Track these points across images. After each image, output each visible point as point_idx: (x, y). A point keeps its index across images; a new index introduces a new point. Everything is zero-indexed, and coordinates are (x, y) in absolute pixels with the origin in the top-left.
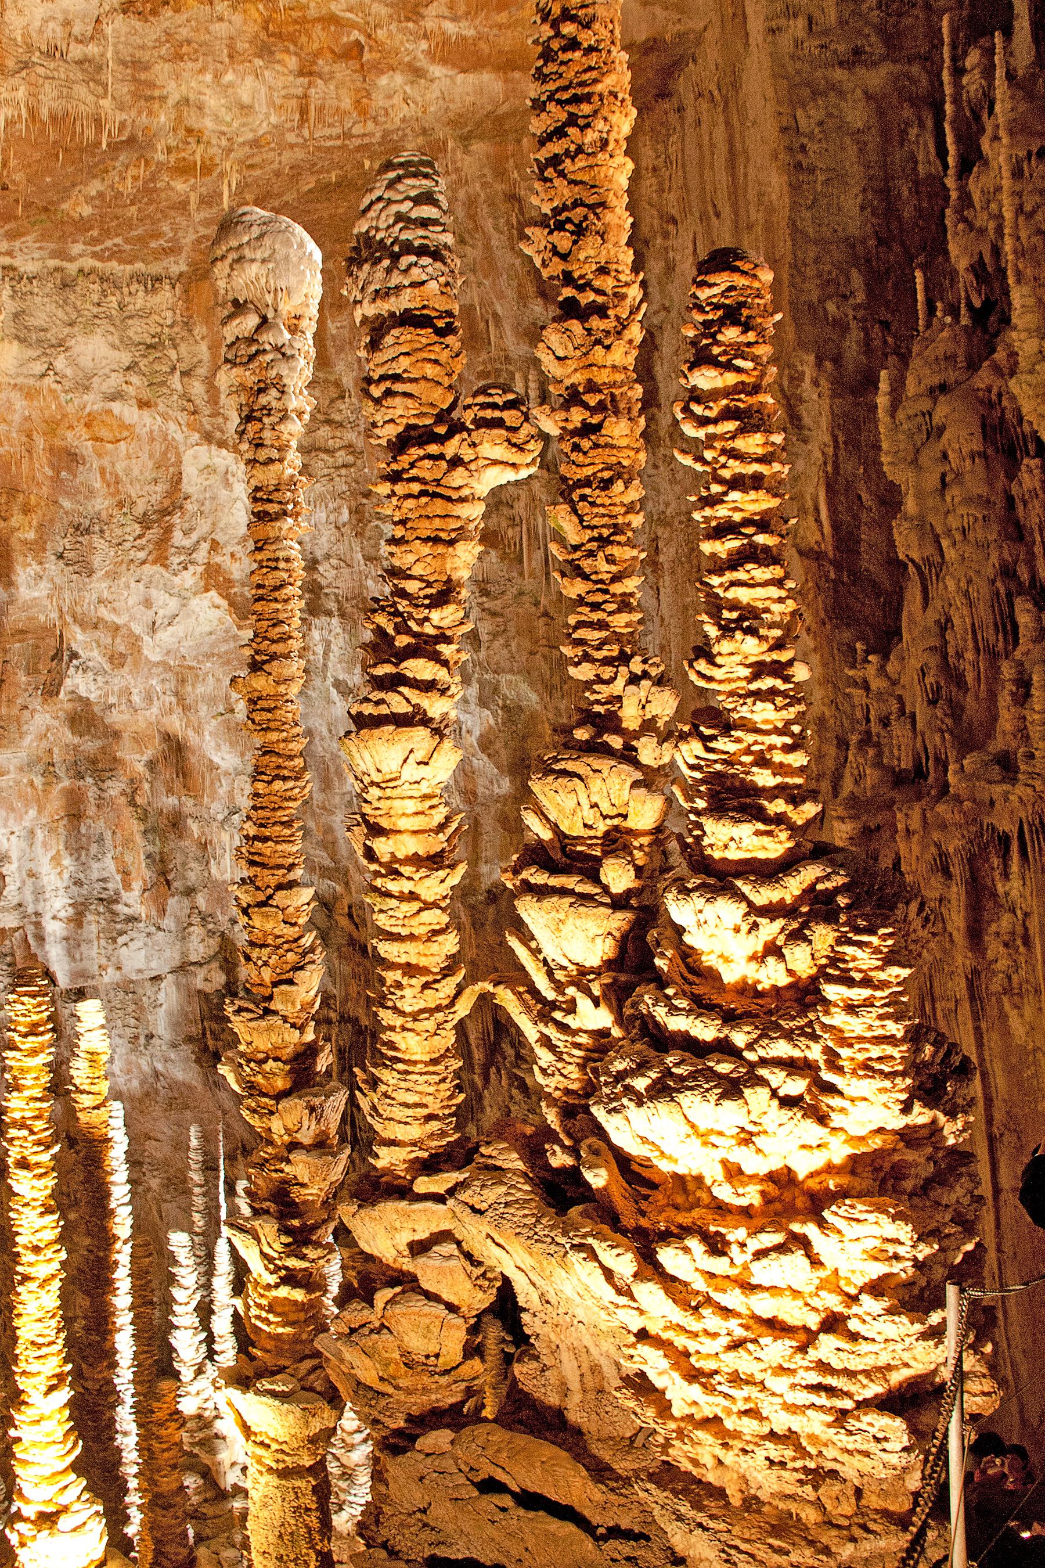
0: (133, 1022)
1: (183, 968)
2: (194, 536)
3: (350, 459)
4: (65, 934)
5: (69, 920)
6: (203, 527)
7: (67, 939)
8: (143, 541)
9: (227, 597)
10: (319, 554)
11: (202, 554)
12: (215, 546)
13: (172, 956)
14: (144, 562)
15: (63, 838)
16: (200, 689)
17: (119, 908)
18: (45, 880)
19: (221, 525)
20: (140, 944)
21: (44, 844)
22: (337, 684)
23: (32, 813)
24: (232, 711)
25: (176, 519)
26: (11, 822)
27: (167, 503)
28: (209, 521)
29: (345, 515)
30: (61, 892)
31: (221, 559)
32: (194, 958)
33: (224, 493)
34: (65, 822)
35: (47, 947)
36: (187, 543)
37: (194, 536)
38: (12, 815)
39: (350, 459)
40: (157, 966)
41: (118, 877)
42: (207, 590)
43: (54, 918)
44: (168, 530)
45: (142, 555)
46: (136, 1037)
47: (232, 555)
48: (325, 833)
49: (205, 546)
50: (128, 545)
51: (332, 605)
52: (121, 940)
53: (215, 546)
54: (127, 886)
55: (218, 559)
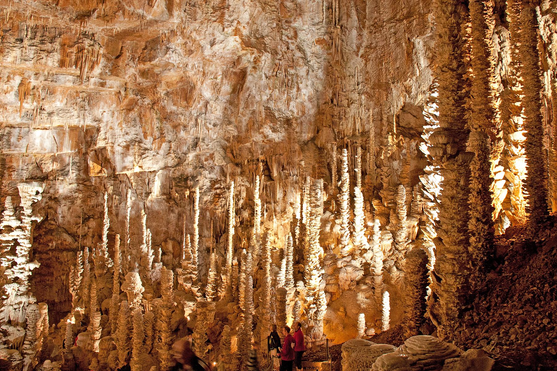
0: (140, 188)
1: (166, 168)
2: (232, 18)
3: (276, 10)
4: (122, 152)
5: (124, 147)
6: (235, 16)
7: (123, 154)
8: (214, 15)
9: (241, 39)
10: (264, 35)
11: (235, 23)
12: (239, 23)
13: (161, 164)
14: (215, 21)
15: (123, 117)
16: (210, 69)
17: (142, 145)
18: (116, 131)
19: (240, 17)
20: (151, 158)
21: (117, 118)
22: (265, 74)
23: (114, 105)
24: (216, 78)
25: (226, 11)
26: (105, 107)
27: (220, 5)
28: (237, 15)
29: (275, 25)
30: (121, 136)
31: (241, 27)
32: (169, 165)
33: (242, 8)
34: (125, 111)
35: (115, 156)
36: (230, 19)
37: (232, 18)
38: (106, 105)
39: (276, 10)
40: (155, 167)
41: (142, 134)
42: (235, 35)
43: (119, 145)
44: (223, 14)
45: (214, 19)
46: (142, 194)
47: (244, 27)
48: (239, 123)
49: (236, 22)
50: (209, 14)
51: (269, 50)
52: (144, 156)
53: (239, 23)
54: (146, 137)
55: (240, 27)
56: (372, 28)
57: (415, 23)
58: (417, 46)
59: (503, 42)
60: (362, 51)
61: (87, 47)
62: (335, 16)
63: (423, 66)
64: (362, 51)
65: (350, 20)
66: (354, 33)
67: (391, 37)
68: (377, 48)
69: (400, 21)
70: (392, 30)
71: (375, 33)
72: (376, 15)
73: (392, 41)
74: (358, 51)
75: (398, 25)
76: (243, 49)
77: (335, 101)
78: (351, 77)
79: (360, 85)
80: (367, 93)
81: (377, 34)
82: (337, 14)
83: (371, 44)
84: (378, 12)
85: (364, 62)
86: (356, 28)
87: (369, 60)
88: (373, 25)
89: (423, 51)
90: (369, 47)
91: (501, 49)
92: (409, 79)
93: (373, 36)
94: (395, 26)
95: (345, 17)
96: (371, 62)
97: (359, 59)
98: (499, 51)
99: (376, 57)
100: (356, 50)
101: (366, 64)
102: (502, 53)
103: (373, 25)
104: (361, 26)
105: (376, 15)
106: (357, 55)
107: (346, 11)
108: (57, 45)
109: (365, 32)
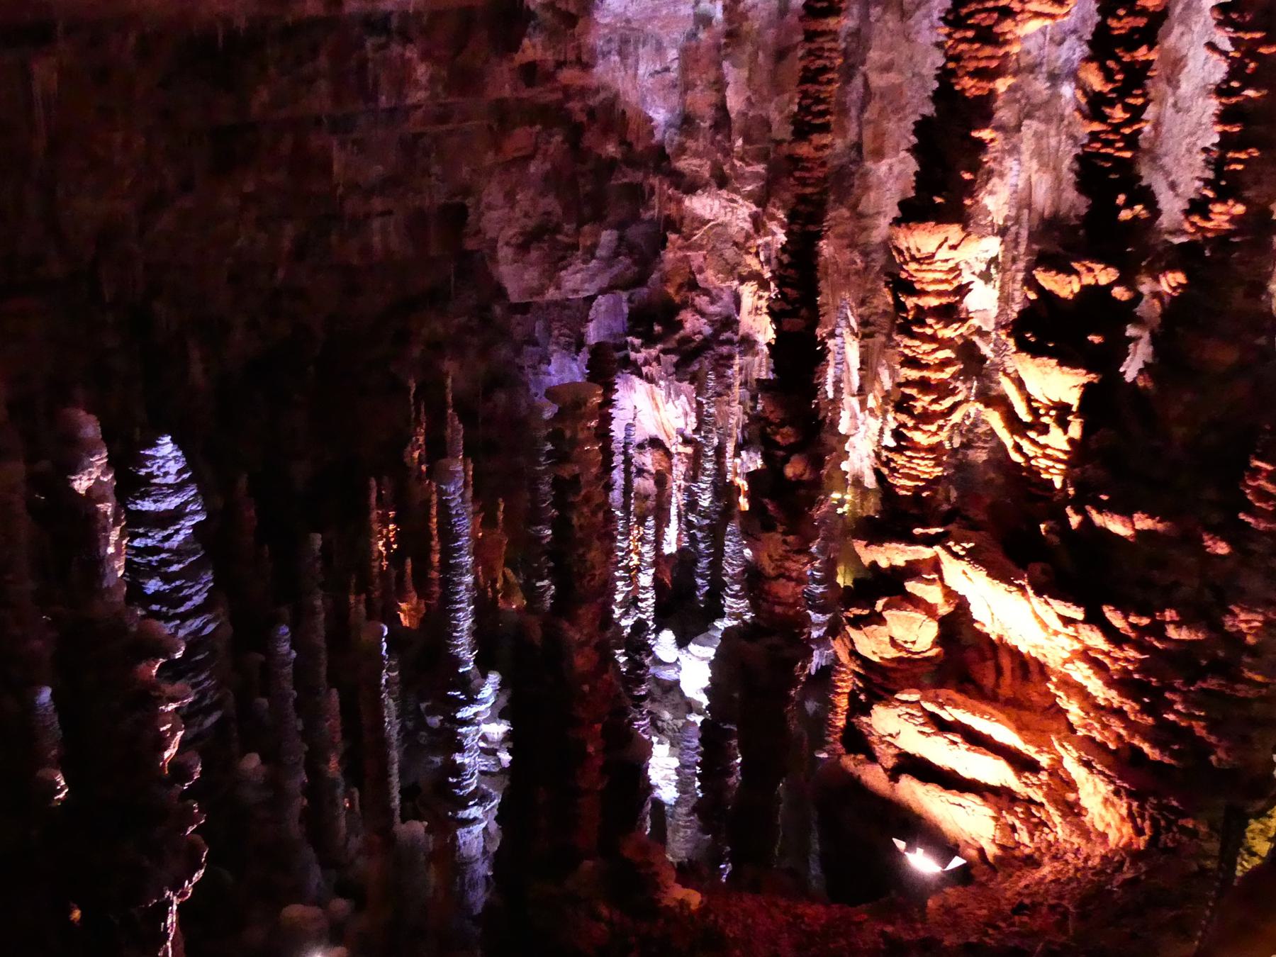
61: (370, 55)
108: (323, 62)
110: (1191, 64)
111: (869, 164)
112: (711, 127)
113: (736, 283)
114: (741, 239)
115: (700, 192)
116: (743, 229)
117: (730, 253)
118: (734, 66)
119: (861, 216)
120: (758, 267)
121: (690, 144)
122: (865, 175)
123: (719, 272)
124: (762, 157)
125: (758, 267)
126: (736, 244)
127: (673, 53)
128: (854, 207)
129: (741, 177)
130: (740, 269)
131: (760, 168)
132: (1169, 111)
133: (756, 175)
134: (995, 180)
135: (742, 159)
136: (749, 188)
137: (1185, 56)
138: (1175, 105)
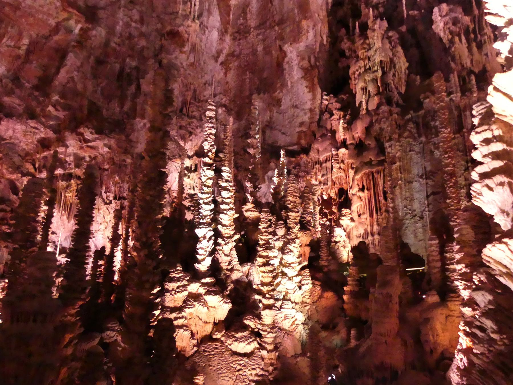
24: (19, 48)
56: (236, 35)
57: (288, 30)
58: (289, 55)
59: (394, 47)
60: (222, 58)
62: (195, 11)
63: (296, 78)
64: (222, 58)
65: (211, 18)
66: (215, 35)
67: (258, 45)
68: (242, 56)
69: (272, 27)
70: (261, 37)
71: (239, 40)
72: (242, 21)
73: (260, 48)
74: (218, 57)
75: (268, 31)
76: (64, 10)
77: (184, 110)
78: (207, 85)
79: (217, 97)
80: (224, 106)
81: (241, 41)
82: (197, 8)
83: (234, 51)
84: (245, 18)
85: (224, 71)
86: (218, 29)
87: (231, 69)
88: (237, 32)
89: (296, 62)
90: (231, 55)
91: (393, 54)
92: (278, 91)
93: (237, 43)
94: (264, 32)
95: (205, 14)
96: (232, 72)
97: (218, 67)
98: (392, 57)
99: (239, 66)
100: (216, 55)
101: (226, 74)
102: (395, 59)
103: (237, 32)
104: (223, 30)
105: (242, 21)
106: (217, 61)
107: (207, 7)
109: (228, 38)
110: (283, 101)
111: (138, 119)
112: (31, 88)
113: (20, 175)
114: (23, 154)
115: (14, 118)
116: (24, 149)
117: (17, 159)
118: (75, 57)
119: (131, 141)
120: (32, 170)
121: (17, 91)
122: (132, 125)
123: (10, 167)
124: (66, 107)
125: (32, 170)
126: (19, 155)
127: (26, 41)
128: (127, 136)
129: (48, 116)
130: (22, 169)
131: (61, 114)
132: (275, 114)
133: (57, 118)
134: (193, 136)
135: (54, 106)
136: (51, 123)
137: (281, 99)
138: (277, 112)
